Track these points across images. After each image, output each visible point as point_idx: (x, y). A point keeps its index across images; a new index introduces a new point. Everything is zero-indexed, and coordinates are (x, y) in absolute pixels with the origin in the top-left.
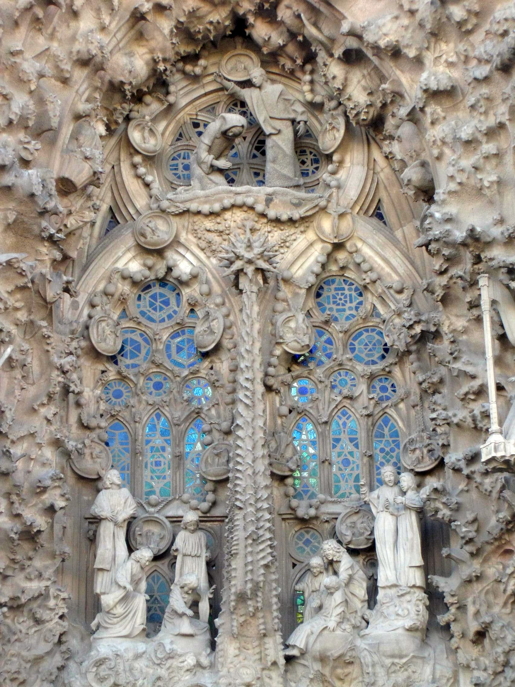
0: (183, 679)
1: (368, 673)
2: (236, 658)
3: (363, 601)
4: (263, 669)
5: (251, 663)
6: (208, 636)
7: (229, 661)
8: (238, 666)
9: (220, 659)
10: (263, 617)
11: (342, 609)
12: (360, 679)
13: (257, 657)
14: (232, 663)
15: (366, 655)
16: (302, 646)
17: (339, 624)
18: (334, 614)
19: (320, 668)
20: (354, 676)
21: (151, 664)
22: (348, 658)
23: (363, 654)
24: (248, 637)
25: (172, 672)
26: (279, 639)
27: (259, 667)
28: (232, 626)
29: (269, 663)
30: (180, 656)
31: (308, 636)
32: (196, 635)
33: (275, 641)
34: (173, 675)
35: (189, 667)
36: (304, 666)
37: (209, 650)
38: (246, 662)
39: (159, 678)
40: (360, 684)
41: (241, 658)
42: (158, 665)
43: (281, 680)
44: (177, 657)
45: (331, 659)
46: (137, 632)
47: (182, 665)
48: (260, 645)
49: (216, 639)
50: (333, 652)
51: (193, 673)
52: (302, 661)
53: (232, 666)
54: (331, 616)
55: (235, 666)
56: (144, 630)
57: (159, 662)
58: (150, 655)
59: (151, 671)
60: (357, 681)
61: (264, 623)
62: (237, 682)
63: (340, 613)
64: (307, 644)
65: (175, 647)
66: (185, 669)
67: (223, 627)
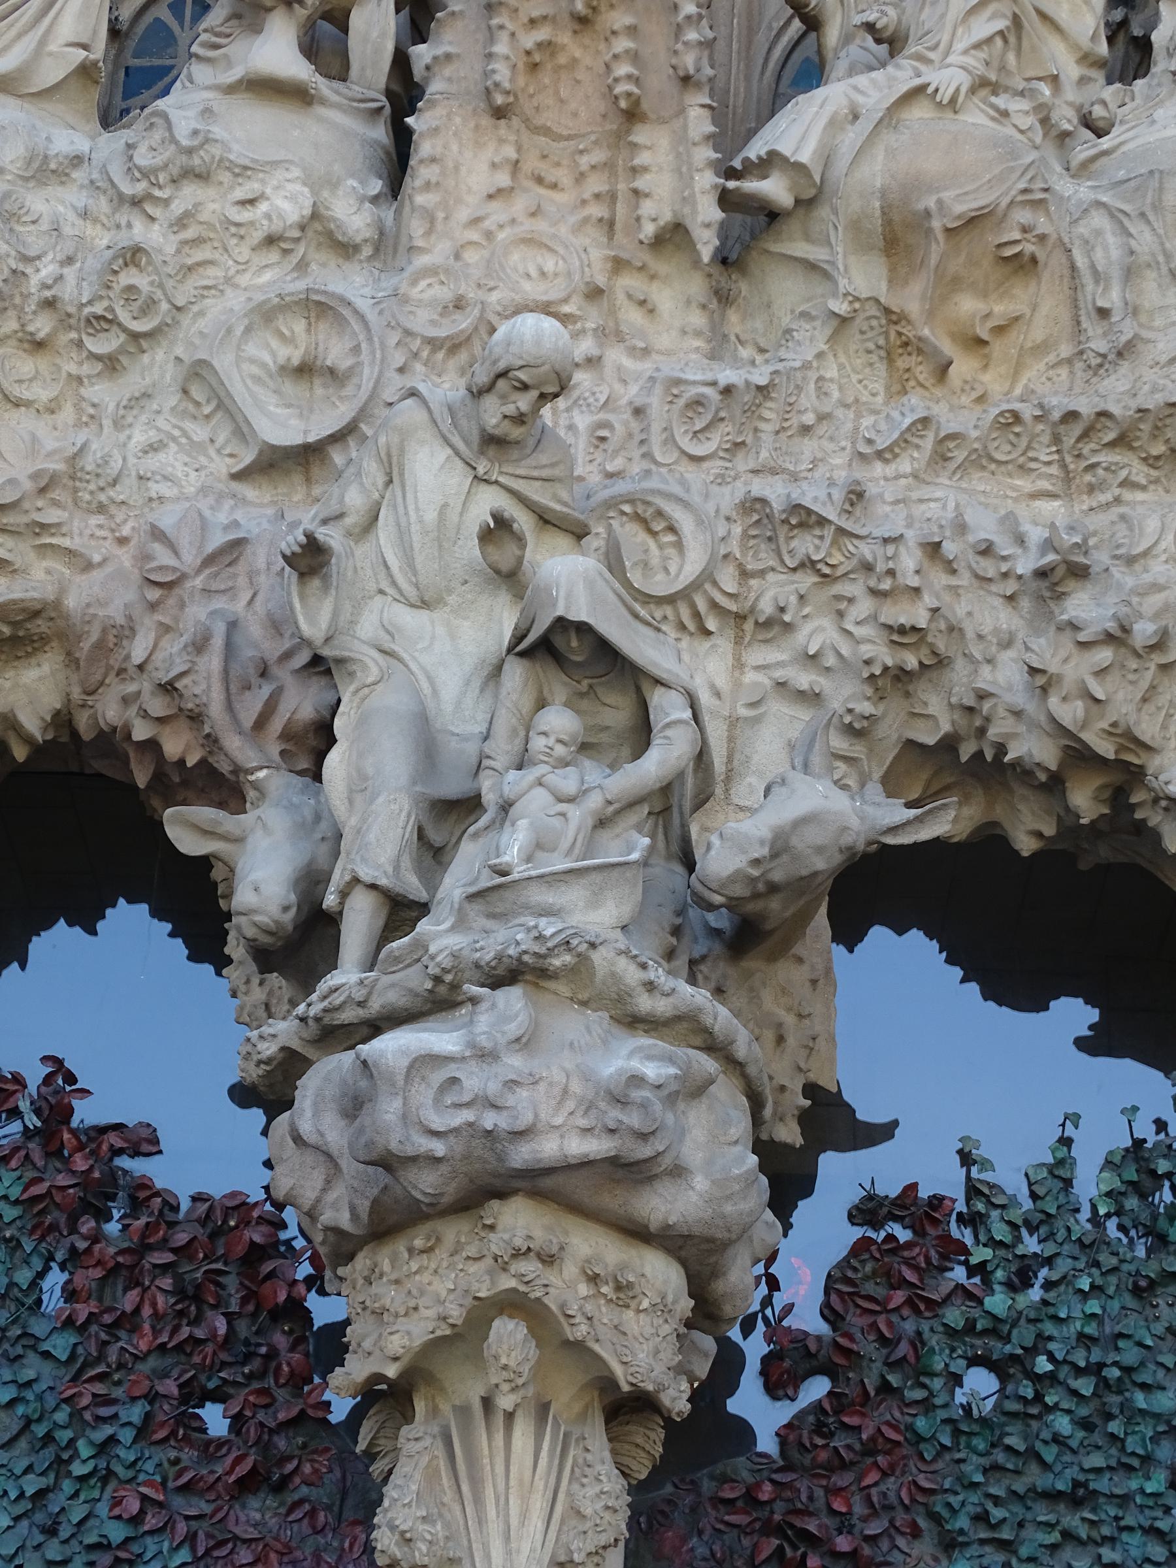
0: (244, 280)
1: (1103, 313)
2: (495, 205)
3: (1086, 59)
4: (618, 265)
5: (563, 230)
6: (380, 133)
7: (463, 214)
8: (501, 236)
9: (420, 199)
10: (632, 30)
11: (1001, 24)
12: (1066, 350)
13: (597, 211)
14: (476, 221)
15: (1098, 233)
16: (804, 157)
17: (981, 84)
18: (959, 46)
19: (882, 290)
20: (1038, 334)
21: (102, 205)
22: (1017, 235)
23: (1082, 229)
24: (558, 138)
25: (198, 242)
26: (699, 122)
27: (597, 255)
28: (490, 56)
29: (649, 230)
30: (243, 171)
31: (834, 125)
32: (323, 102)
33: (681, 139)
34: (199, 255)
35: (276, 227)
36: (811, 267)
37: (376, 186)
38: (541, 226)
39: (133, 256)
40: (1064, 372)
41: (520, 205)
42: (136, 202)
43: (698, 319)
44: (225, 177)
45: (936, 224)
46: (52, 73)
47: (245, 215)
48: (608, 166)
49: (409, 120)
50: (947, 195)
51: (294, 259)
52: (801, 249)
53: (474, 235)
54: (947, 53)
55: (489, 235)
56: (85, 71)
57: (141, 187)
58: (104, 171)
59: (102, 239)
60: (1051, 358)
61: (634, 57)
62: (494, 297)
63: (989, 40)
64: (827, 158)
65: (217, 131)
66: (258, 236)
67: (448, 71)
